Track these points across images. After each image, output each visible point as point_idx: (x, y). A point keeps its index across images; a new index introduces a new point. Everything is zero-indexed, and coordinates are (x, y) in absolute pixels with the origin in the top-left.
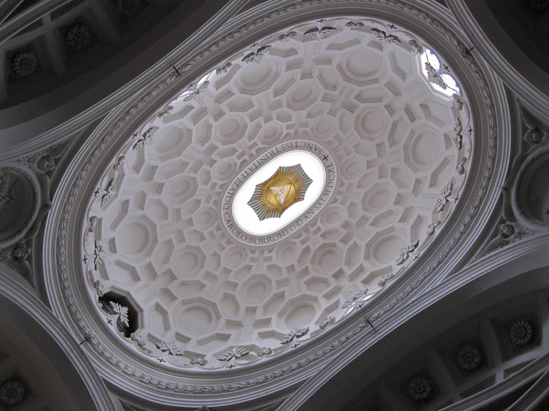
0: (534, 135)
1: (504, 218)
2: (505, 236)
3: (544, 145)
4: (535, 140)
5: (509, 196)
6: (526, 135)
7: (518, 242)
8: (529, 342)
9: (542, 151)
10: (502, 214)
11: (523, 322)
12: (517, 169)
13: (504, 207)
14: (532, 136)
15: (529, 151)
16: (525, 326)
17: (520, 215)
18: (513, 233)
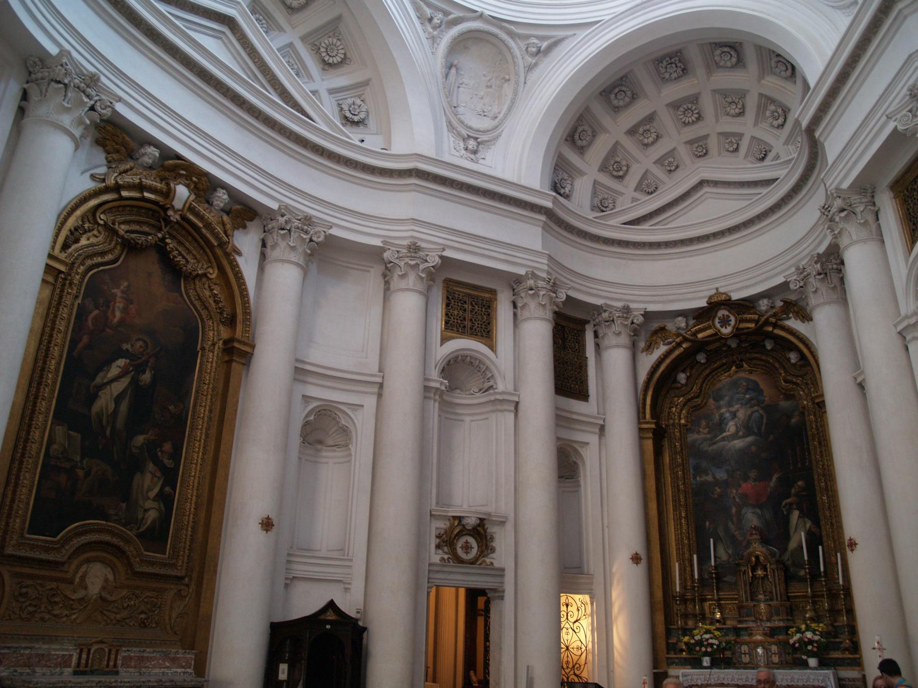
0: (534, 50)
1: (451, 17)
2: (430, 20)
3: (523, 58)
4: (529, 49)
5: (474, 19)
6: (536, 41)
7: (423, 36)
8: (324, 61)
9: (517, 58)
10: (456, 14)
11: (343, 52)
12: (502, 28)
13: (461, 15)
14: (534, 47)
15: (519, 42)
16: (339, 55)
17: (452, 36)
18: (435, 28)
